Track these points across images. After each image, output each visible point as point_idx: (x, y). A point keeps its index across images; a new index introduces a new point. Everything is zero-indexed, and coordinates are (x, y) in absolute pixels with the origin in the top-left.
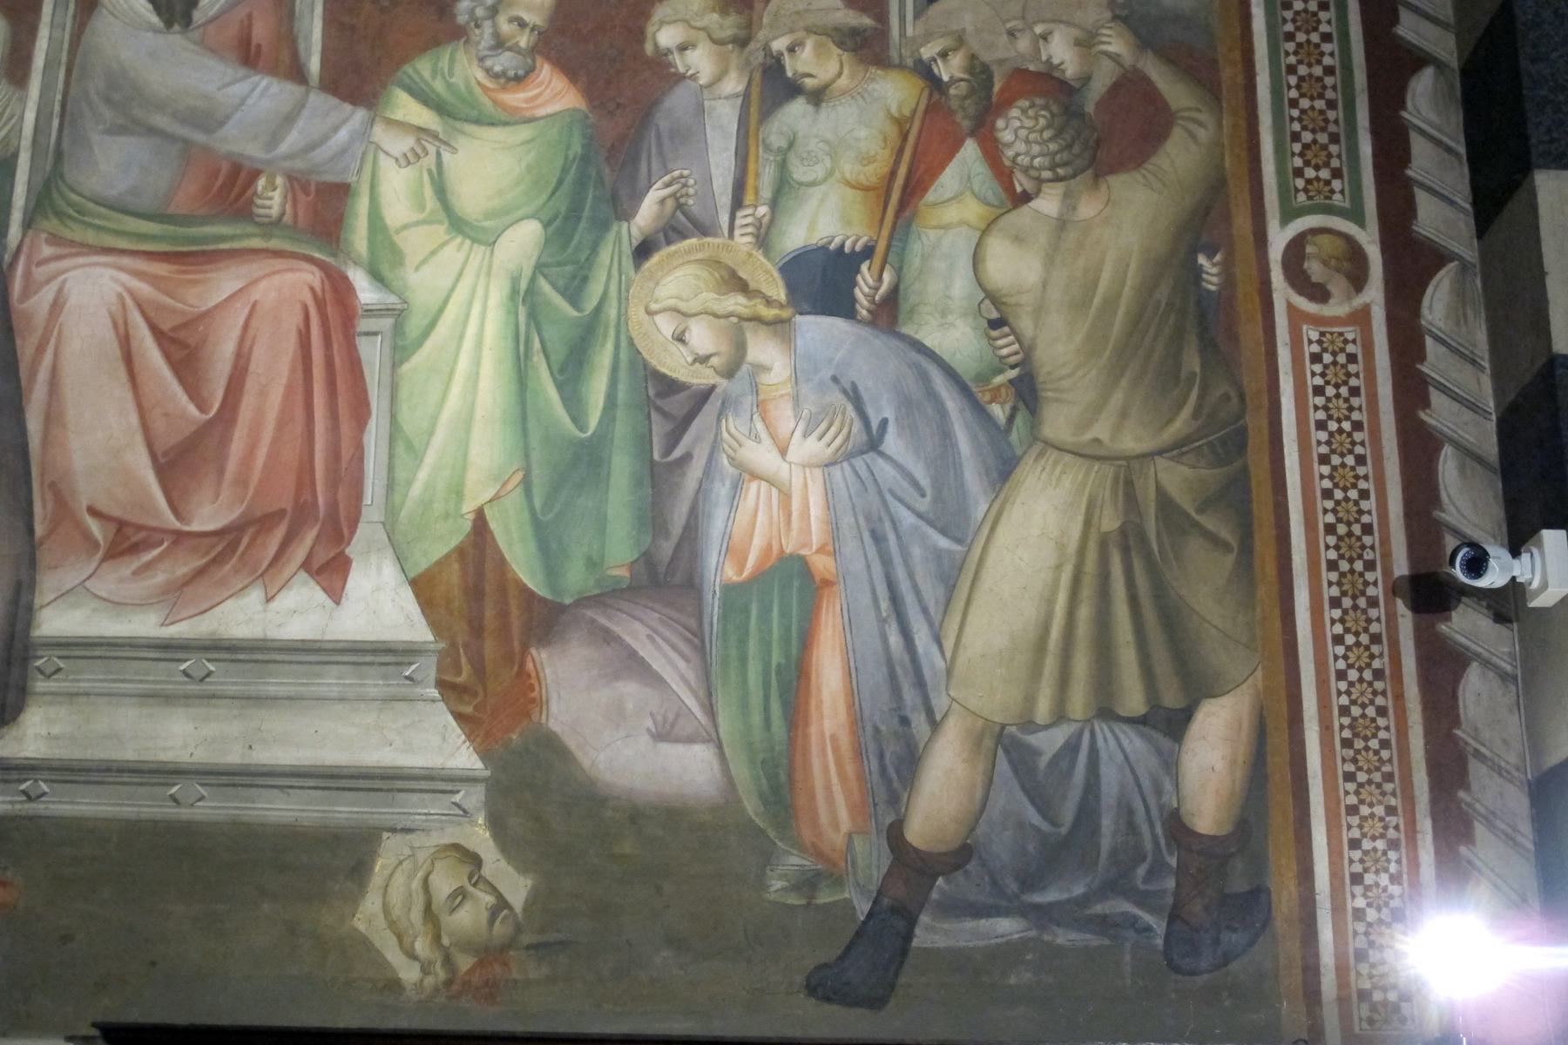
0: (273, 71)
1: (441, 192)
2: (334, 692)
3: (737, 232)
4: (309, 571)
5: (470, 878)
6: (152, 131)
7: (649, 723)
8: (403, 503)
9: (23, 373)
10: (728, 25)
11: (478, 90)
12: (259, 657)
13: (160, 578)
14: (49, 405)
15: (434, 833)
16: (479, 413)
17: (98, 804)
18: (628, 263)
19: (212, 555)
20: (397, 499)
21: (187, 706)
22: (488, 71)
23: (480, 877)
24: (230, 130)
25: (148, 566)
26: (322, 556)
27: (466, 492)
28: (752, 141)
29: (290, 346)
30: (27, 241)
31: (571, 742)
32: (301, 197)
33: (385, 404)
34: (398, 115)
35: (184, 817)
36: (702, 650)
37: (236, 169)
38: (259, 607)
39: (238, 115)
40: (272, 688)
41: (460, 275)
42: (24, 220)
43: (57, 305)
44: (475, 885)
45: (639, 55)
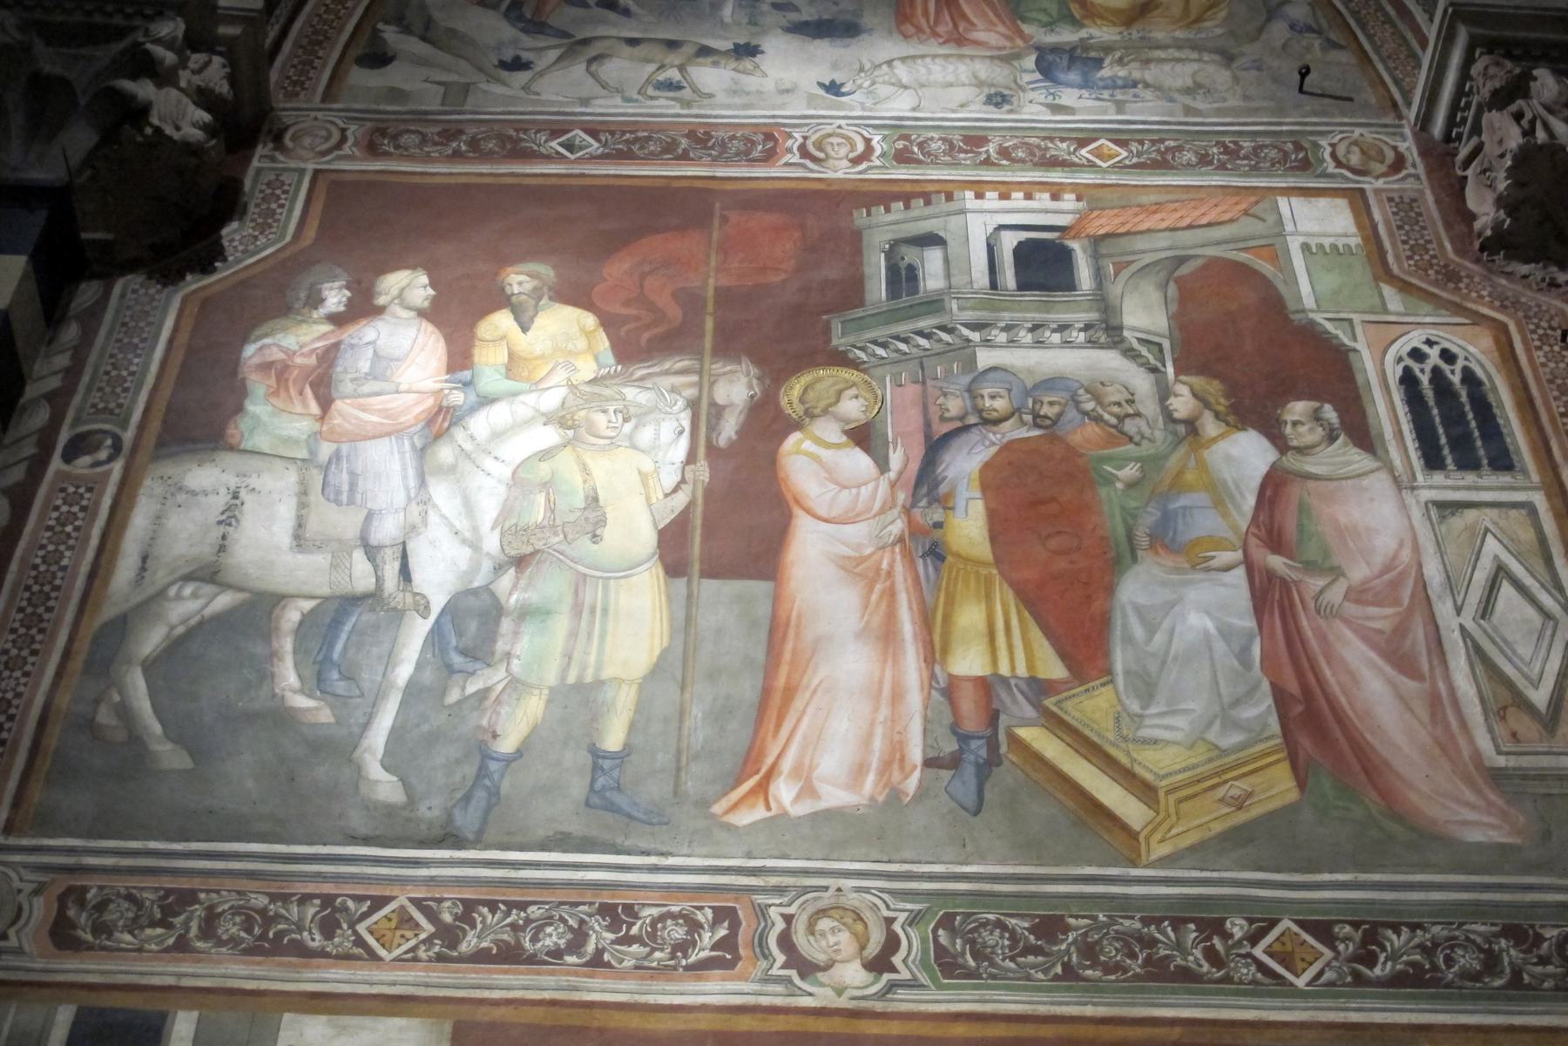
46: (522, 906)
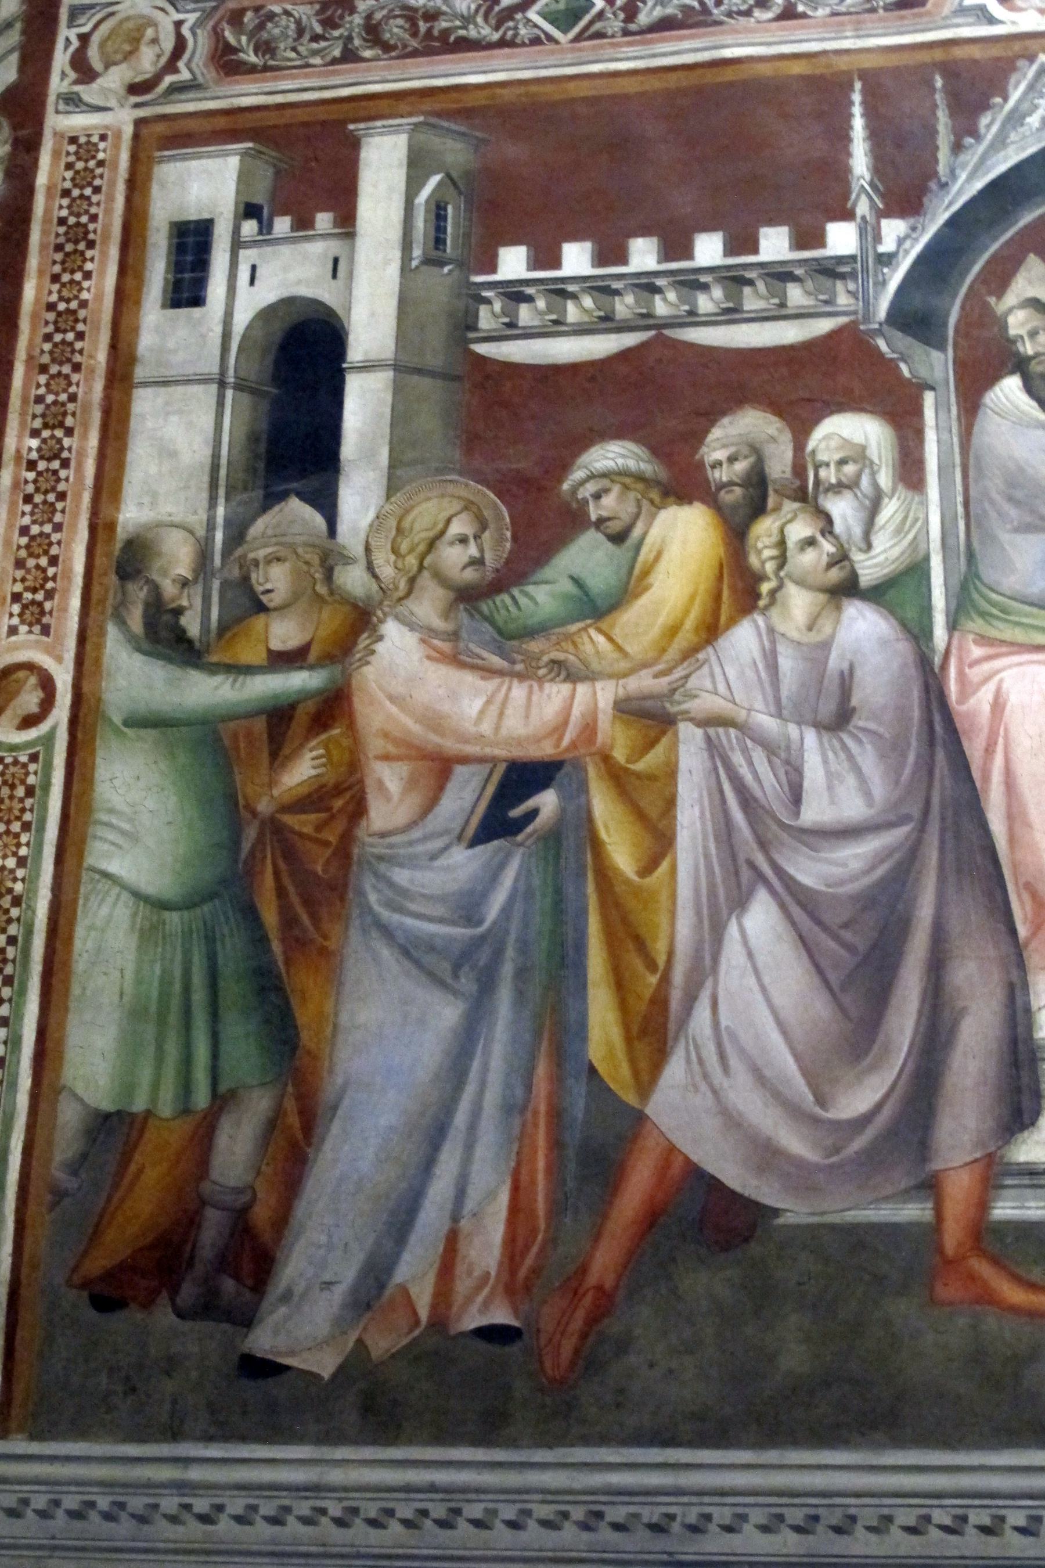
9: (976, 774)
14: (1009, 806)
30: (955, 642)
42: (947, 622)
43: (998, 705)
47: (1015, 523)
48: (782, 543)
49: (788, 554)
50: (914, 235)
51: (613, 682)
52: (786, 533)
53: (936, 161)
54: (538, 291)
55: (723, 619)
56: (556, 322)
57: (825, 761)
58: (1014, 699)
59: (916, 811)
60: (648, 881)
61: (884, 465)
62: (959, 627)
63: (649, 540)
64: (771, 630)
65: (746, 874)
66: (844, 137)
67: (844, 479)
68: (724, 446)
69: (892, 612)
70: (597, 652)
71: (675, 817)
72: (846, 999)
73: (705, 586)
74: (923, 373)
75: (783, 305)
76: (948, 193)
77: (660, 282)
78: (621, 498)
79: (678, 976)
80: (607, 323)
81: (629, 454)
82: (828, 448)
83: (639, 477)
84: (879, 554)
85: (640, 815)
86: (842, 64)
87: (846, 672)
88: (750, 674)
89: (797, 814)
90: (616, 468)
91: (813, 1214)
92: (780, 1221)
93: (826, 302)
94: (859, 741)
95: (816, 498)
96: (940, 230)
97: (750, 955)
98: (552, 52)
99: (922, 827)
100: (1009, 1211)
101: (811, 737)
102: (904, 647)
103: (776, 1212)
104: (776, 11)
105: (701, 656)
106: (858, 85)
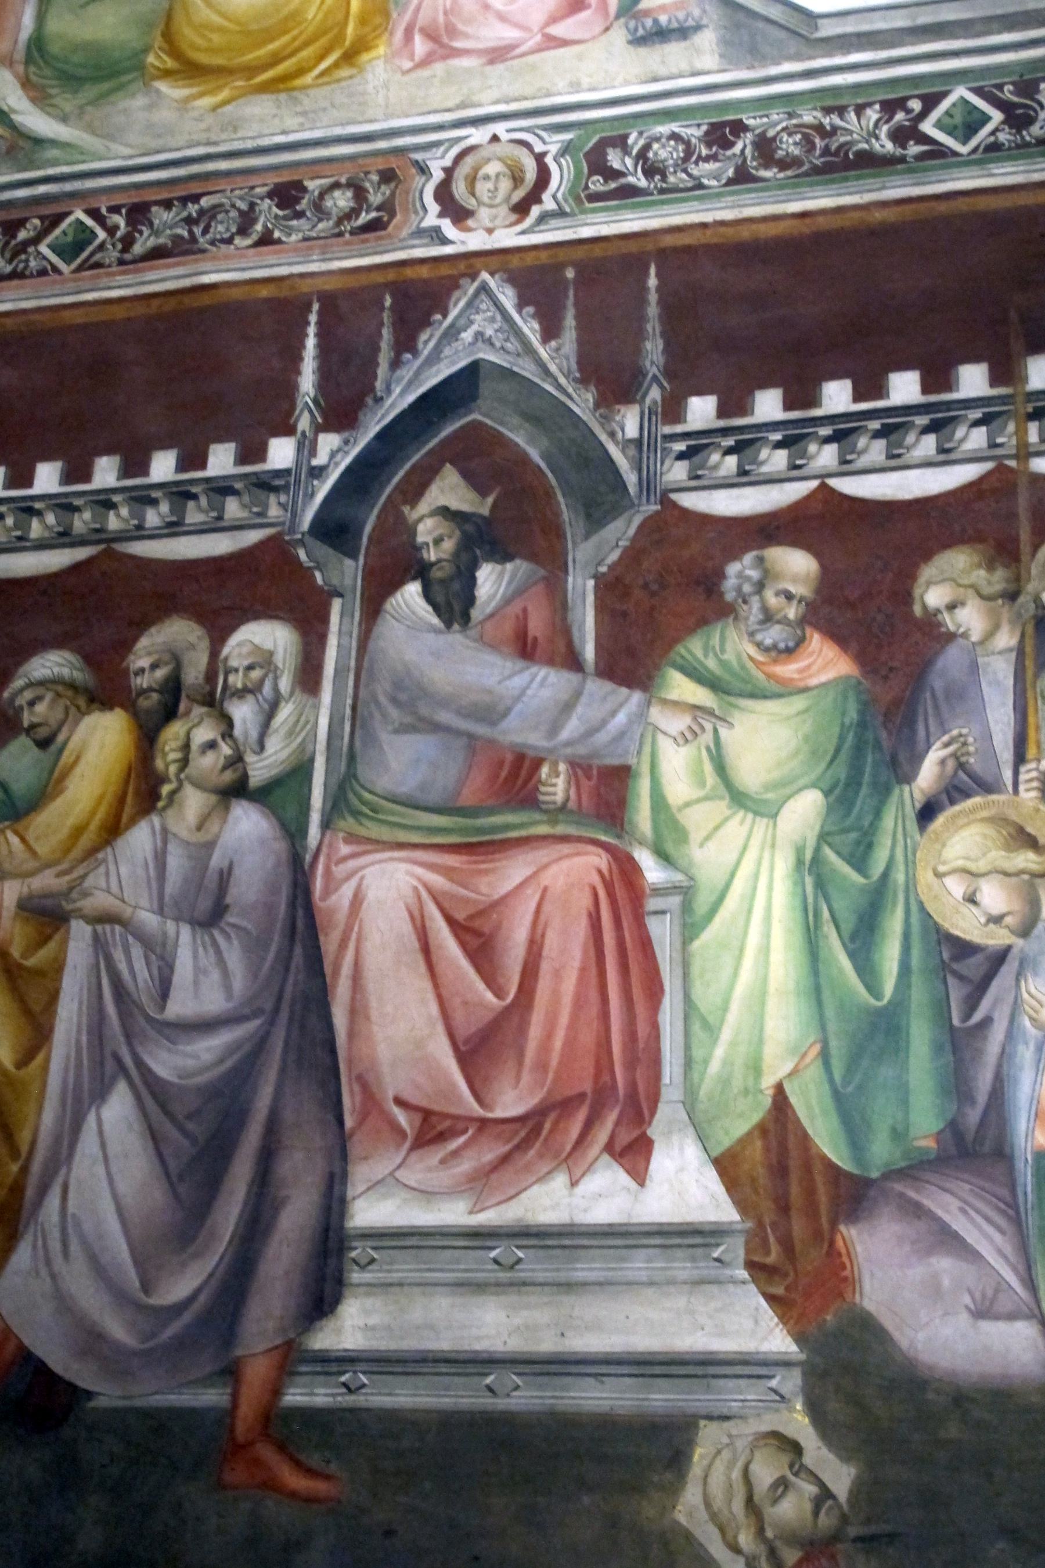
0: (551, 662)
1: (721, 768)
2: (643, 1276)
3: (1022, 788)
4: (612, 1154)
5: (791, 1466)
6: (437, 728)
7: (967, 1300)
8: (702, 1080)
9: (328, 969)
10: (997, 580)
11: (750, 665)
12: (567, 1242)
13: (466, 1166)
14: (353, 999)
15: (751, 1421)
16: (773, 986)
17: (415, 1395)
18: (912, 825)
19: (516, 1141)
20: (696, 1076)
21: (497, 1294)
22: (759, 645)
23: (802, 1465)
24: (511, 722)
25: (455, 1154)
26: (625, 1137)
27: (764, 1068)
28: (1030, 694)
29: (581, 929)
30: (326, 841)
31: (888, 1322)
32: (585, 783)
33: (678, 983)
34: (673, 695)
35: (500, 1407)
36: (1017, 1221)
37: (520, 758)
38: (565, 1192)
39: (519, 707)
40: (580, 1274)
41: (745, 848)
42: (322, 821)
43: (357, 900)
44: (796, 1474)
45: (909, 616)
46: (196, 198)
47: (396, 725)
48: (186, 747)
49: (191, 756)
50: (346, 449)
51: (20, 881)
52: (191, 736)
53: (375, 377)
54: (9, 509)
55: (125, 819)
56: (20, 538)
57: (195, 957)
58: (372, 894)
59: (268, 1006)
60: (23, 1072)
61: (286, 672)
62: (332, 826)
63: (71, 745)
64: (165, 831)
65: (110, 1065)
66: (295, 358)
67: (249, 685)
68: (149, 654)
69: (274, 813)
70: (10, 852)
71: (55, 1012)
72: (182, 1189)
73: (113, 789)
74: (335, 581)
75: (220, 518)
76: (381, 407)
77: (116, 498)
78: (53, 703)
79: (36, 1167)
80: (64, 538)
81: (64, 662)
82: (240, 655)
83: (72, 686)
84: (271, 756)
85: (26, 1011)
86: (305, 287)
87: (225, 871)
88: (140, 872)
89: (162, 1008)
90: (51, 676)
91: (124, 1398)
92: (92, 1404)
93: (259, 515)
94: (228, 937)
95: (222, 701)
96: (369, 444)
97: (103, 1145)
98: (54, 282)
99: (272, 1022)
100: (298, 1398)
101: (186, 932)
102: (281, 846)
103: (89, 1395)
104: (255, 237)
105: (100, 856)
106: (316, 307)
